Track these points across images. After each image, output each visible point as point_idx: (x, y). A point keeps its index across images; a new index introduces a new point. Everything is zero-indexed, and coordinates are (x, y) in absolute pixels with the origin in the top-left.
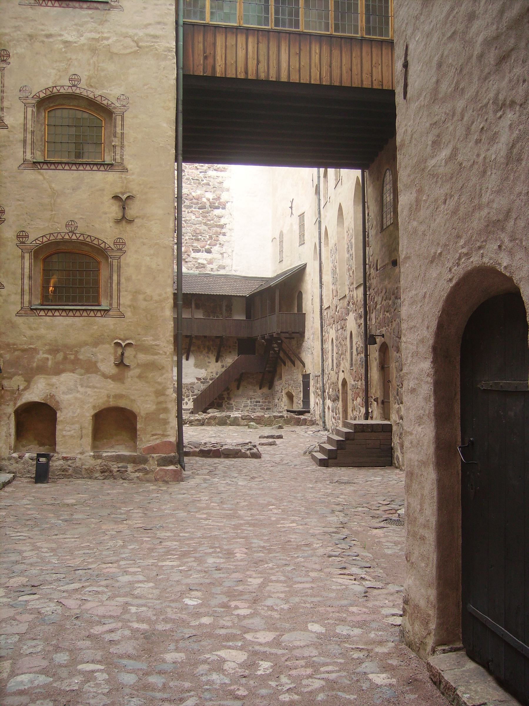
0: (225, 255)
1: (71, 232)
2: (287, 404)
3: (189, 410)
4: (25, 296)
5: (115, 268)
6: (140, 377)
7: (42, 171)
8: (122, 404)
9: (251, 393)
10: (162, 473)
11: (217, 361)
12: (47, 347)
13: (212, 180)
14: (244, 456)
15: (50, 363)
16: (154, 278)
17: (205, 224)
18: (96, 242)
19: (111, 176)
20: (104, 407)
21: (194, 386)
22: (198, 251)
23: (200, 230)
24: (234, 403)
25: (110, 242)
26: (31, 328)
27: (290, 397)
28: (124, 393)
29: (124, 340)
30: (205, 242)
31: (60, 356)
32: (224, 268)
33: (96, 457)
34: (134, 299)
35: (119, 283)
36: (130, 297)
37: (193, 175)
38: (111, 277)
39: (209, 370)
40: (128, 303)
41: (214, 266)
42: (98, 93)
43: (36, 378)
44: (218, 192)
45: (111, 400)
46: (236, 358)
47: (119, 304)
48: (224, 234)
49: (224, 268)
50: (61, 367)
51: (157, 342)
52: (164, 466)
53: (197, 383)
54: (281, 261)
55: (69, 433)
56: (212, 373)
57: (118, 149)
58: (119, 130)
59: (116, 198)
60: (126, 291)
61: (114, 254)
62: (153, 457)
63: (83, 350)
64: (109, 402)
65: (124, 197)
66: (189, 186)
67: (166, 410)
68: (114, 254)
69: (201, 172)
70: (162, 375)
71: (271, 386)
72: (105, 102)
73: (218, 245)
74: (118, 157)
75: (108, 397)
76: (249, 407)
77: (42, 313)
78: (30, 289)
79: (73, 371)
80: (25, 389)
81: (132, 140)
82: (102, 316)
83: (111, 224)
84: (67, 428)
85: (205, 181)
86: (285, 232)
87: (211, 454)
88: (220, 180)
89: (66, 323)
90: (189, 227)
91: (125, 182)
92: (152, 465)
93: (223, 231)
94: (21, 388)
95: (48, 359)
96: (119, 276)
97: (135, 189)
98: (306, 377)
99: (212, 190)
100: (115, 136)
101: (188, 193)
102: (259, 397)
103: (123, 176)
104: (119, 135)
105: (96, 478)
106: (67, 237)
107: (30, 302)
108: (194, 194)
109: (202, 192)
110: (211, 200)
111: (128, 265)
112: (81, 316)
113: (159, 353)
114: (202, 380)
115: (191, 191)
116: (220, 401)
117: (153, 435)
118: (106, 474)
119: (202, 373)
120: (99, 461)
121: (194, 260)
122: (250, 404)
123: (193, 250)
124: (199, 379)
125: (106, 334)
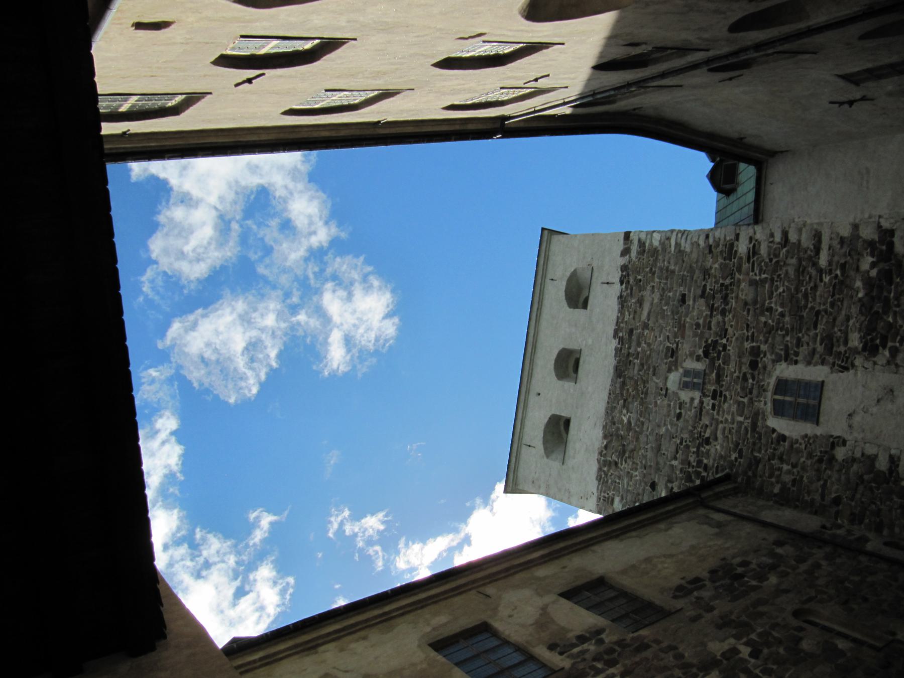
13: (836, 258)
37: (826, 295)
44: (860, 245)
66: (845, 304)
69: (821, 280)
85: (838, 272)
88: (836, 243)
99: (856, 257)
101: (859, 304)
109: (859, 277)
110: (874, 260)
115: (855, 299)
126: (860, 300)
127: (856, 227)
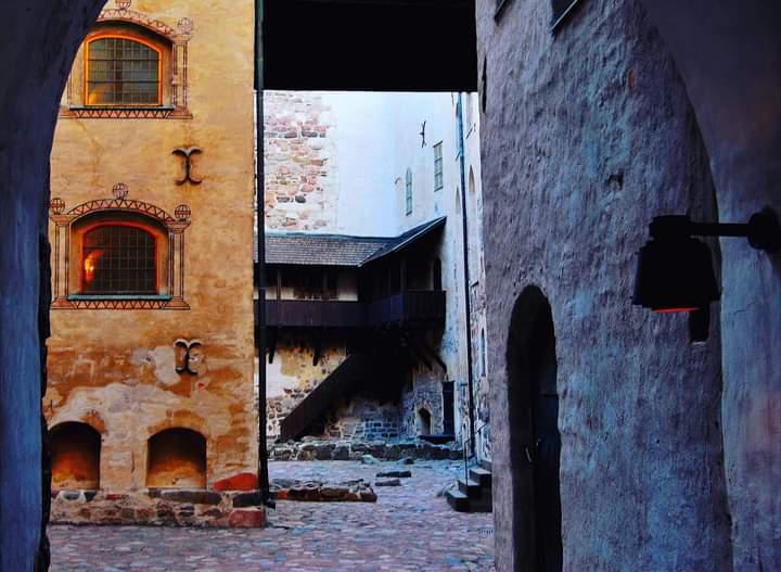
0: (325, 205)
1: (119, 198)
2: (420, 427)
3: (274, 437)
4: (60, 284)
5: (177, 245)
6: (210, 388)
7: (81, 120)
8: (187, 423)
9: (367, 412)
10: (239, 517)
11: (315, 364)
12: (89, 350)
14: (353, 498)
15: (92, 371)
16: (228, 258)
17: (296, 160)
18: (151, 211)
19: (171, 125)
20: (162, 428)
24: (341, 427)
25: (170, 211)
26: (67, 325)
27: (425, 415)
28: (189, 409)
29: (189, 340)
31: (105, 362)
33: (154, 494)
34: (202, 285)
35: (182, 265)
36: (196, 283)
38: (172, 258)
39: (304, 378)
40: (195, 290)
41: (310, 222)
42: (153, 17)
43: (74, 390)
44: (315, 112)
45: (172, 419)
46: (344, 358)
47: (182, 293)
49: (325, 225)
50: (107, 375)
51: (233, 342)
52: (242, 506)
54: (409, 213)
55: (116, 464)
57: (180, 89)
58: (180, 65)
59: (178, 152)
60: (191, 274)
61: (176, 226)
62: (228, 496)
63: (135, 352)
64: (169, 421)
65: (188, 152)
67: (244, 432)
68: (176, 226)
70: (238, 385)
71: (397, 400)
72: (162, 29)
74: (180, 100)
75: (169, 414)
77: (82, 305)
78: (67, 274)
79: (122, 381)
80: (61, 404)
81: (197, 77)
82: (160, 308)
83: (173, 187)
84: (115, 457)
86: (414, 171)
87: (306, 496)
89: (113, 317)
90: (272, 164)
91: (190, 131)
92: (227, 505)
93: (323, 169)
94: (55, 403)
95: (89, 365)
96: (182, 255)
97: (201, 141)
98: (449, 387)
100: (176, 74)
102: (379, 417)
103: (187, 125)
104: (180, 71)
105: (153, 525)
106: (114, 205)
107: (67, 291)
108: (278, 116)
109: (291, 113)
111: (194, 241)
112: (133, 308)
113: (235, 357)
114: (293, 393)
115: (274, 111)
117: (229, 465)
118: (166, 518)
119: (293, 382)
120: (157, 500)
124: (288, 391)
125: (165, 332)
126: (274, 116)
127: (328, 109)
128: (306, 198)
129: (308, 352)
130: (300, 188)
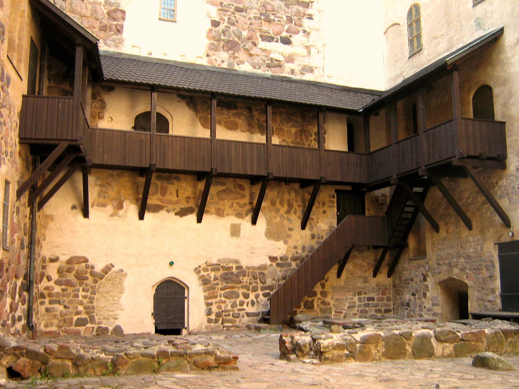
0: (313, 50)
21: (265, 272)
22: (271, 39)
23: (273, 6)
30: (280, 26)
32: (311, 70)
39: (291, 243)
48: (310, 17)
53: (271, 265)
56: (295, 247)
73: (301, 33)
76: (356, 309)
93: (309, 11)
102: (373, 290)
114: (279, 261)
116: (310, 299)
119: (280, 249)
121: (264, 54)
122: (357, 303)
123: (261, 36)
124: (273, 259)
128: (291, 39)
129: (295, 213)
130: (286, 27)
